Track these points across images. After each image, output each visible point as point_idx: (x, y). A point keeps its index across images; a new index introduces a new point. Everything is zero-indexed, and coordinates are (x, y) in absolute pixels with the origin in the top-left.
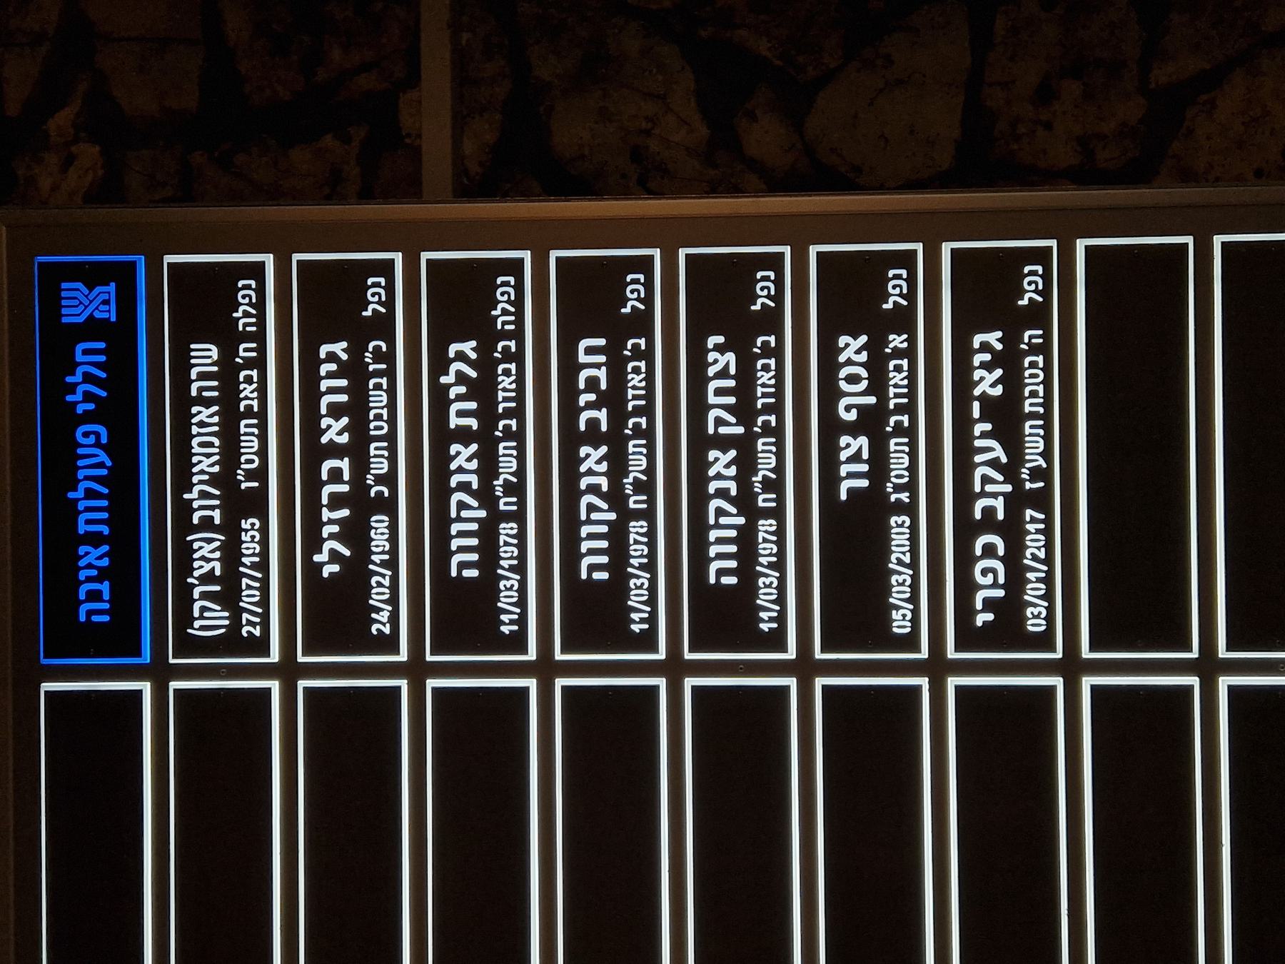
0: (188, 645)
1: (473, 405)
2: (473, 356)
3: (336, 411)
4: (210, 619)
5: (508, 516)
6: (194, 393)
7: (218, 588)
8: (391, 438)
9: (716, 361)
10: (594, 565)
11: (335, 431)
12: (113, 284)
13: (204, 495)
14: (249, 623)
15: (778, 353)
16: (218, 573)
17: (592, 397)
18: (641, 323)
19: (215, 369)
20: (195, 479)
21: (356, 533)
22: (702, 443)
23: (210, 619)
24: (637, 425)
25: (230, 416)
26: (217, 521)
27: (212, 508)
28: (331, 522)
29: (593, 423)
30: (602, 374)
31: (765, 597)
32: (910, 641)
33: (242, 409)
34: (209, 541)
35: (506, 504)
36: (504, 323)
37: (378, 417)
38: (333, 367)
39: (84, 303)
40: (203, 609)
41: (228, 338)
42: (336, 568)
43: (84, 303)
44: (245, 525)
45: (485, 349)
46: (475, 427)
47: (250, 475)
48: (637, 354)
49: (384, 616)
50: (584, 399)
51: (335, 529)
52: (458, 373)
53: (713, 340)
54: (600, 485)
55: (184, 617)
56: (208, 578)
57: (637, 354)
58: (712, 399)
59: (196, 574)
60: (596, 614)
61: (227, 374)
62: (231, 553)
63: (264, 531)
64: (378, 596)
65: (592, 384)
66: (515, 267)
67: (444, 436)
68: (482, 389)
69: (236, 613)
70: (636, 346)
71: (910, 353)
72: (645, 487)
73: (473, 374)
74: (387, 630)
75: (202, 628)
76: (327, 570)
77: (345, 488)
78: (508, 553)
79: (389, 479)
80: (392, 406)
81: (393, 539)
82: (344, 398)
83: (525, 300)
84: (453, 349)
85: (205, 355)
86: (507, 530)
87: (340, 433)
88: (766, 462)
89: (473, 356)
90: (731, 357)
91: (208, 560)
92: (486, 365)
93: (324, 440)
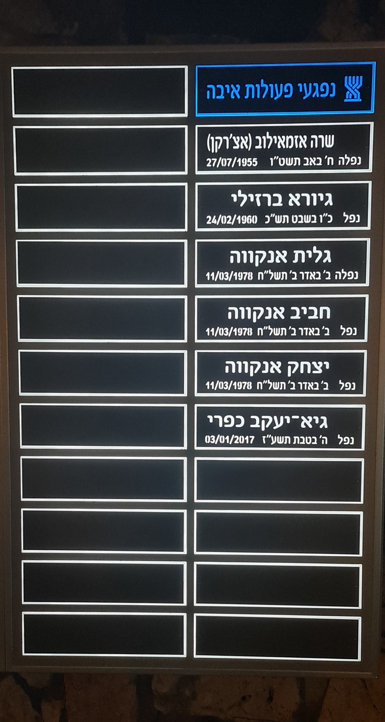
0: (203, 133)
1: (303, 261)
2: (325, 261)
3: (303, 200)
4: (214, 144)
5: (255, 276)
6: (313, 137)
7: (228, 147)
8: (291, 225)
9: (318, 365)
10: (234, 313)
11: (294, 199)
12: (361, 100)
13: (268, 141)
14: (212, 162)
15: (321, 391)
16: (234, 147)
17: (305, 313)
18: (336, 334)
19: (323, 146)
20: (275, 137)
21: (250, 208)
23: (214, 144)
24: (293, 332)
25: (301, 153)
26: (257, 147)
27: (262, 145)
28: (255, 198)
29: (294, 313)
30: (315, 317)
31: (220, 384)
32: (201, 443)
33: (305, 158)
34: (248, 143)
36: (338, 275)
37: (299, 219)
38: (322, 199)
39: (353, 86)
40: (219, 141)
41: (335, 152)
42: (235, 200)
43: (353, 86)
44: (255, 160)
45: (327, 266)
46: (294, 262)
47: (276, 162)
48: (323, 332)
49: (214, 221)
50: (304, 309)
51: (252, 200)
52: (317, 254)
53: (327, 364)
54: (268, 316)
55: (215, 132)
56: (232, 143)
57: (323, 332)
58: (302, 363)
59: (234, 138)
60: (214, 313)
61: (320, 152)
62: (243, 153)
63: (252, 168)
64: (223, 219)
65: (311, 313)
66: (362, 279)
67: (290, 248)
68: (310, 265)
69: (217, 155)
70: (326, 332)
71: (319, 445)
73: (316, 261)
74: (208, 223)
75: (211, 141)
76: (234, 196)
77: (269, 204)
78: (240, 276)
79: (273, 224)
80: (304, 225)
81: (247, 225)
82: (308, 204)
84: (328, 252)
85: (329, 142)
86: (250, 275)
87: (293, 202)
88: (276, 386)
89: (325, 261)
90: (320, 371)
91: (240, 143)
92: (321, 267)
93: (290, 195)
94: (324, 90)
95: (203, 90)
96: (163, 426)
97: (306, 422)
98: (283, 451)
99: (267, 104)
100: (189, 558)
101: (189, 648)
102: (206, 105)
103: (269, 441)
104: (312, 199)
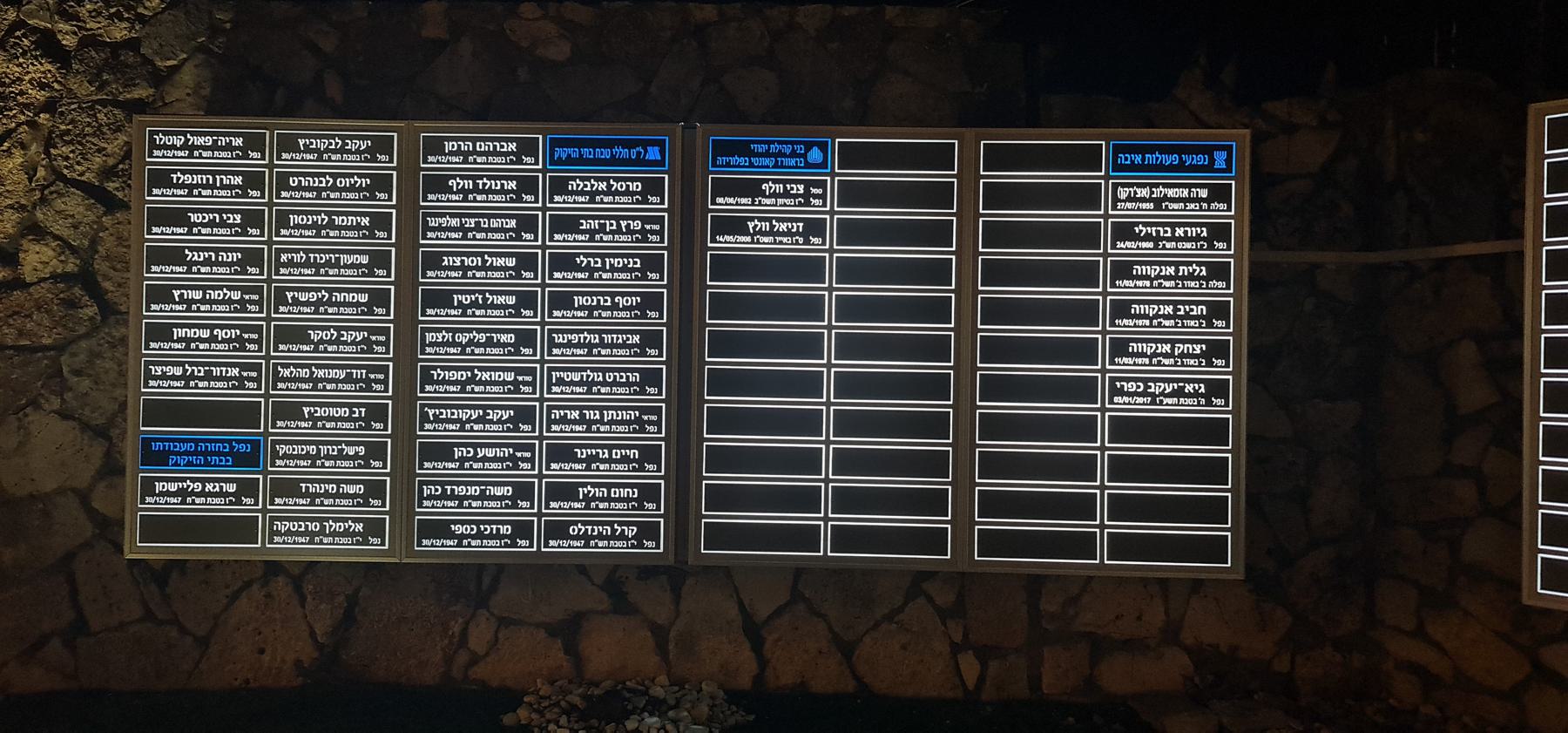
0: (1115, 186)
4: (1123, 193)
11: (1180, 232)
18: (1210, 325)
21: (1148, 237)
22: (1173, 342)
23: (1123, 193)
31: (1125, 360)
35: (1155, 283)
39: (1220, 158)
41: (1209, 200)
45: (1203, 278)
55: (1124, 185)
60: (1121, 309)
61: (1198, 200)
62: (1143, 200)
64: (1128, 244)
67: (1177, 265)
68: (1191, 277)
72: (1160, 325)
78: (1140, 283)
79: (1164, 248)
83: (1220, 290)
86: (1148, 283)
88: (1166, 361)
92: (1199, 278)
94: (1201, 160)
95: (1115, 157)
96: (1083, 390)
97: (1189, 388)
98: (1172, 408)
99: (1160, 168)
100: (1102, 488)
101: (1103, 557)
102: (1118, 167)
103: (1161, 403)
104: (1192, 232)
